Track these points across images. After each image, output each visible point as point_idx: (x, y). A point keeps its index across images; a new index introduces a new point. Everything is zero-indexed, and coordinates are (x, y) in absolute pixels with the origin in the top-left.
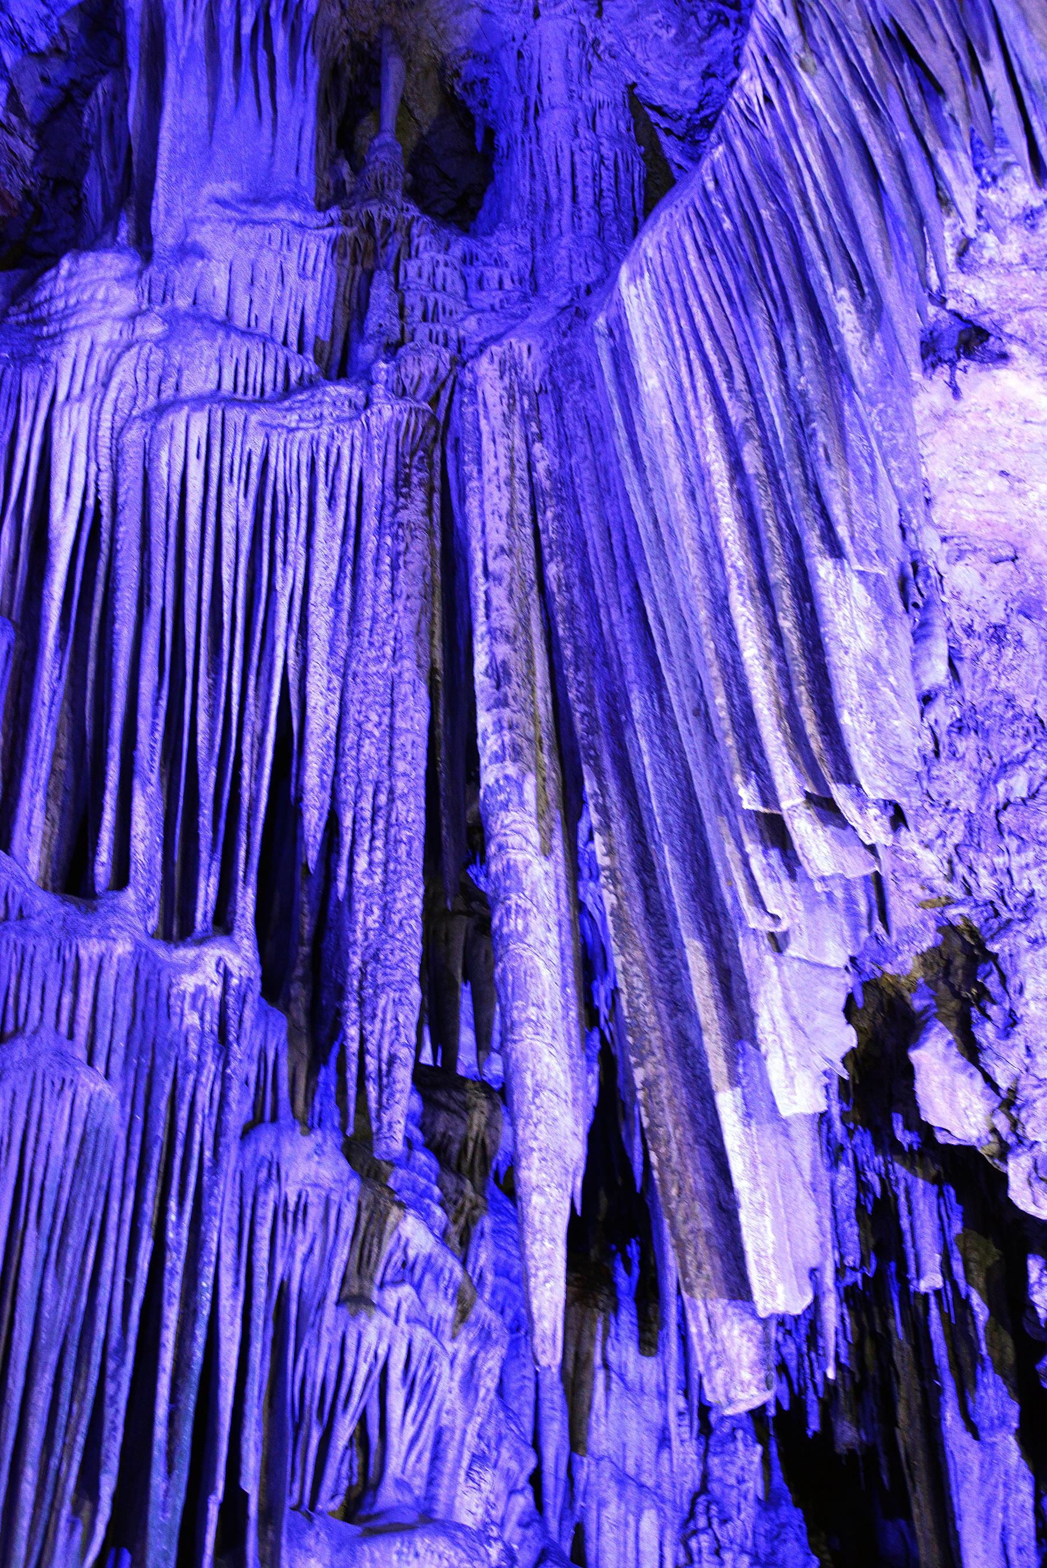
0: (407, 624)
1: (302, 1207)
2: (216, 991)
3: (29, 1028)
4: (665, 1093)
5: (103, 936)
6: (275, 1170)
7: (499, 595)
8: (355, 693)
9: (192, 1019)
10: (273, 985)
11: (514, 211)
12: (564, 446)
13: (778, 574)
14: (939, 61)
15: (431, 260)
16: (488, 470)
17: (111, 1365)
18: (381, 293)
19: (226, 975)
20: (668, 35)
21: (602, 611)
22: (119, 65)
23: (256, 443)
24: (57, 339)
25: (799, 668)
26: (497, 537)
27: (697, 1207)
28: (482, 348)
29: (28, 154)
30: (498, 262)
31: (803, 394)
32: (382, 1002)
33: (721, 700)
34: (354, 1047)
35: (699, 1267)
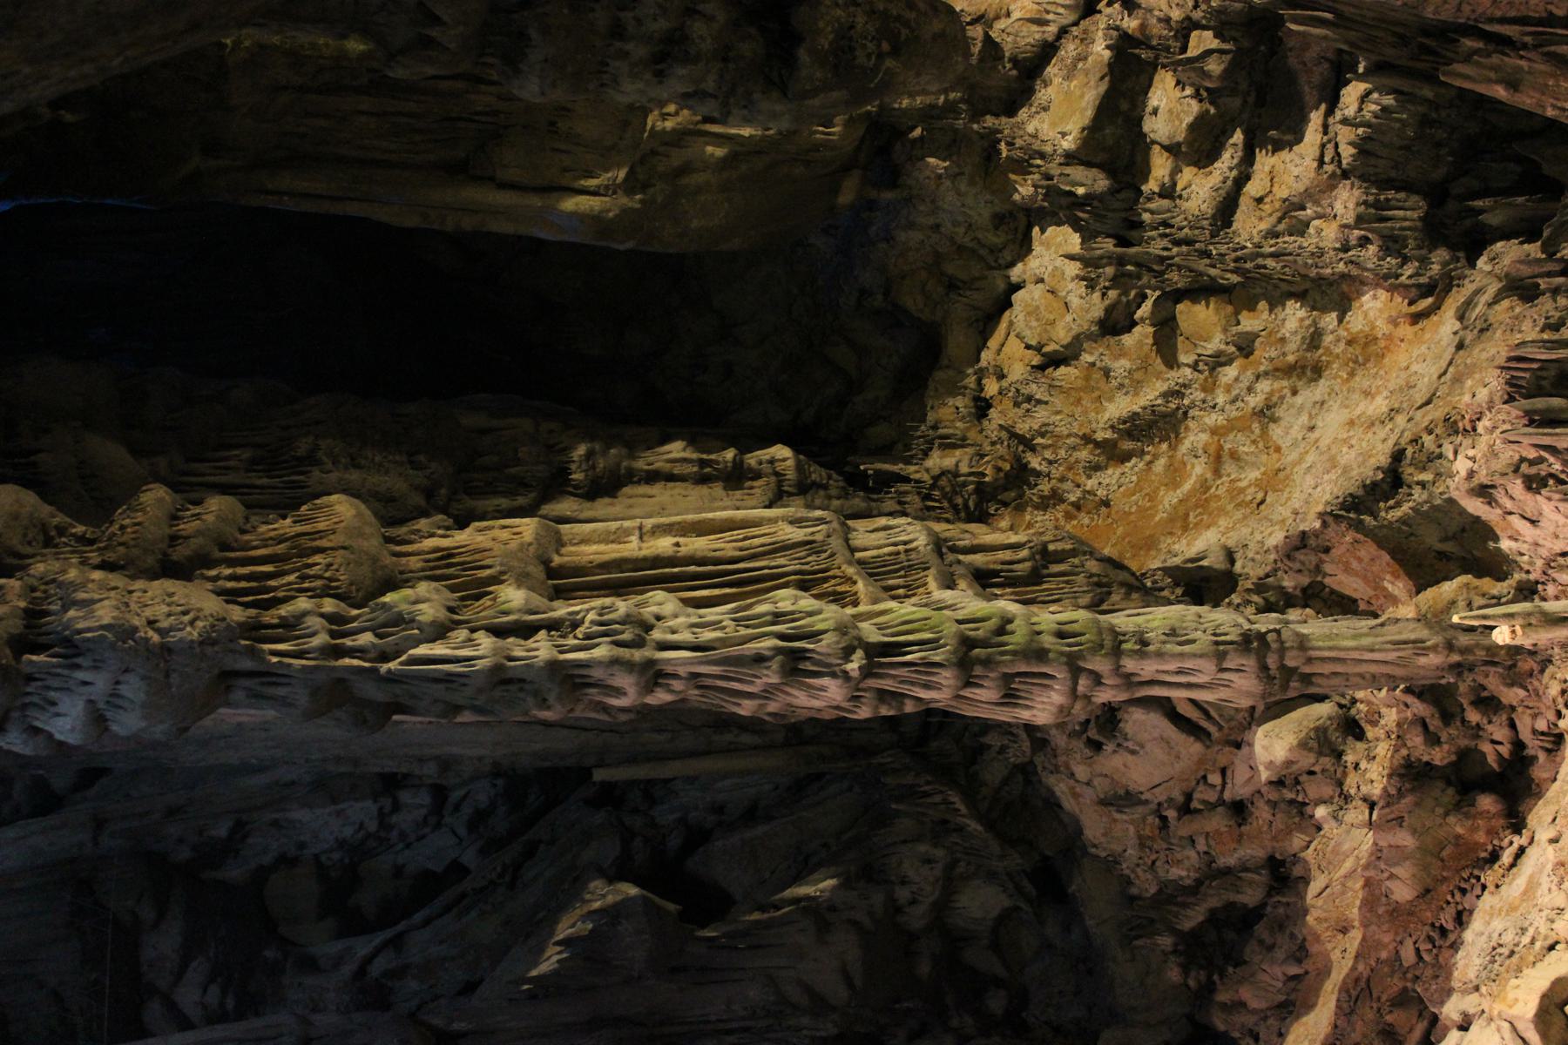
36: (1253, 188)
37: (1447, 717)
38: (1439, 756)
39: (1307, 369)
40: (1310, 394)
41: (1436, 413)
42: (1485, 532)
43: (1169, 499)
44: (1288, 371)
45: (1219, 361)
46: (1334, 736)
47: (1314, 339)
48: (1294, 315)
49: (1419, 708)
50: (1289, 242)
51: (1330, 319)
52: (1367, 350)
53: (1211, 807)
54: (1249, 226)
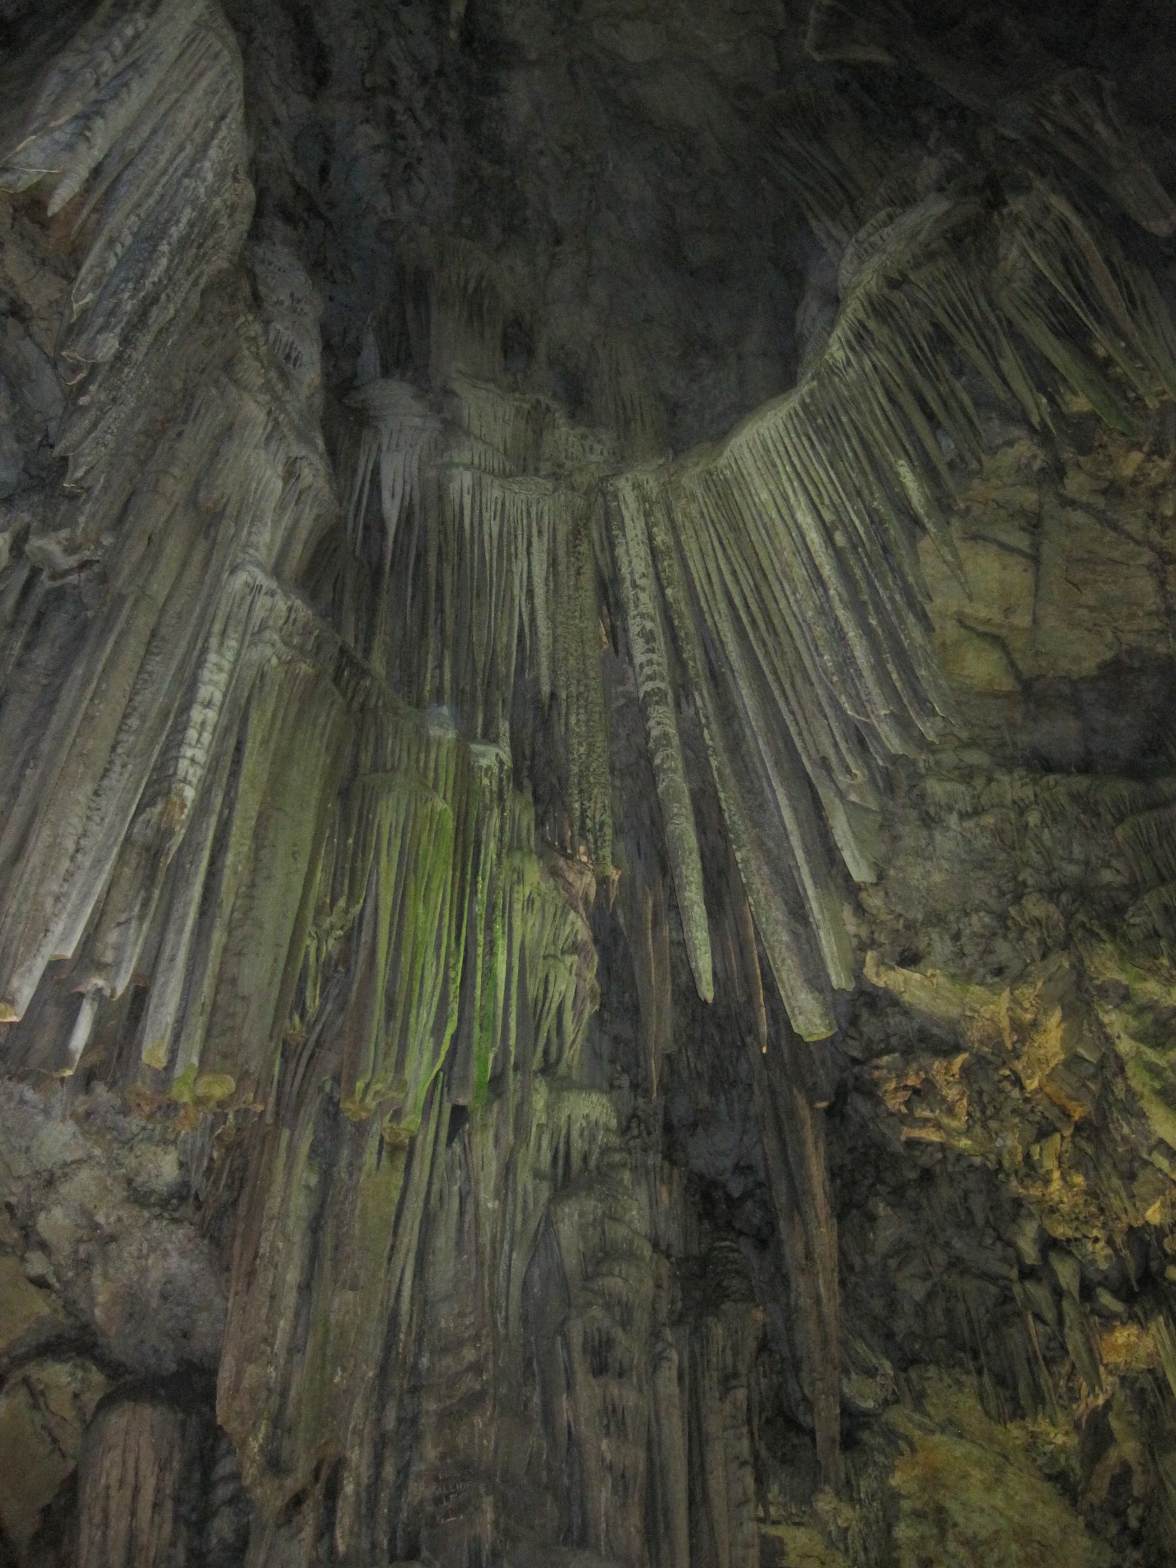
2: (496, 770)
3: (403, 767)
4: (754, 868)
9: (486, 782)
16: (630, 534)
17: (452, 961)
19: (501, 763)
21: (707, 616)
27: (780, 928)
31: (876, 510)
32: (596, 791)
34: (578, 813)
35: (783, 960)
39: (939, 1517)
40: (956, 1512)
47: (919, 1515)
48: (903, 1531)
51: (906, 1505)
52: (932, 1480)
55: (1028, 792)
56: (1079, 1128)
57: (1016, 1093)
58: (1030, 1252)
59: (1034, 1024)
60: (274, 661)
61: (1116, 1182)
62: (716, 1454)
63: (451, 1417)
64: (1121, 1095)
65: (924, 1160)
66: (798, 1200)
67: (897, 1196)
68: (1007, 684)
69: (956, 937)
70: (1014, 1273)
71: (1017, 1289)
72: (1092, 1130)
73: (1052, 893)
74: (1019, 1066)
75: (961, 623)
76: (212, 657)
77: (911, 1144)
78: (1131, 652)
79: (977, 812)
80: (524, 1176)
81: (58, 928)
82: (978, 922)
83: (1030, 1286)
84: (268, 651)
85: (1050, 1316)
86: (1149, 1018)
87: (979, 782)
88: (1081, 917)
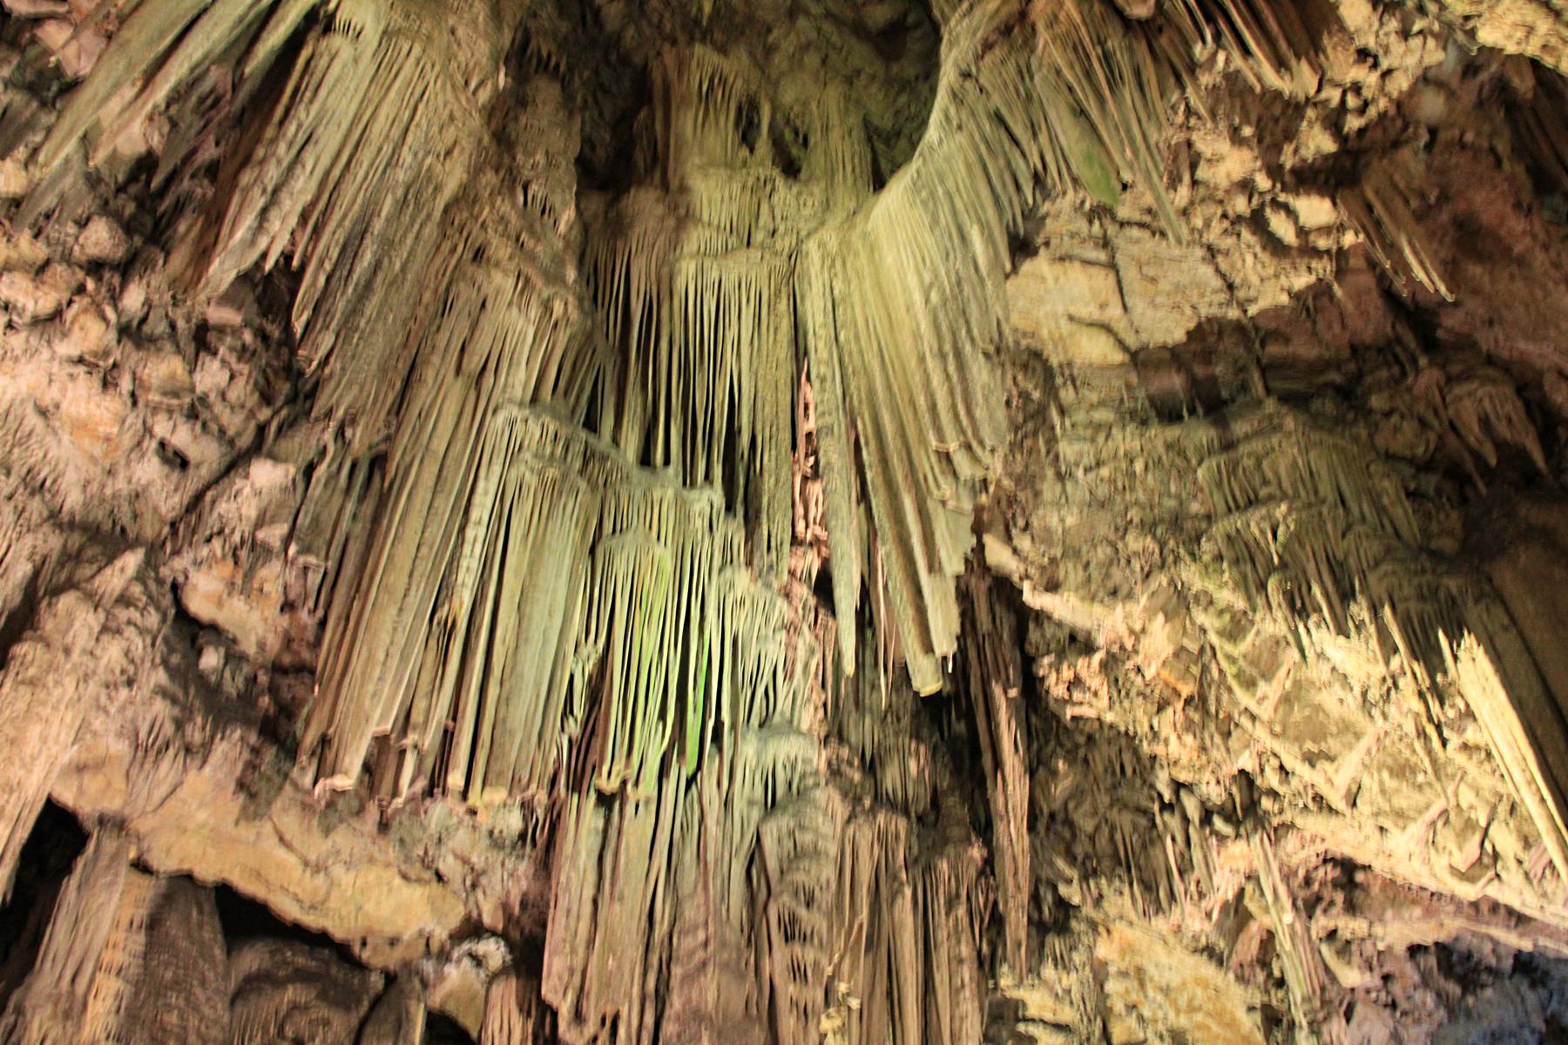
0: (782, 356)
1: (743, 602)
5: (663, 486)
6: (732, 585)
7: (821, 345)
8: (760, 384)
9: (699, 522)
10: (730, 507)
11: (818, 173)
12: (847, 281)
13: (948, 347)
14: (1019, 131)
15: (784, 193)
18: (765, 208)
20: (880, 97)
22: (650, 100)
23: (715, 275)
24: (631, 225)
25: (958, 390)
26: (820, 319)
28: (809, 235)
29: (608, 137)
30: (812, 195)
33: (922, 398)
36: (1048, 1016)
37: (1319, 899)
38: (1339, 897)
40: (1151, 970)
41: (1171, 940)
42: (1225, 907)
43: (1215, 1028)
44: (1142, 985)
45: (1141, 1019)
46: (1339, 944)
47: (1124, 974)
48: (1112, 986)
49: (1319, 911)
50: (1076, 996)
51: (1112, 969)
52: (1127, 949)
53: (1388, 993)
54: (1067, 1015)
55: (1137, 444)
56: (1188, 701)
57: (1139, 679)
58: (1167, 796)
59: (1143, 630)
60: (528, 474)
61: (1218, 739)
62: (941, 957)
63: (688, 979)
64: (1215, 674)
65: (1087, 729)
66: (998, 764)
67: (1071, 757)
68: (1118, 357)
69: (1087, 565)
70: (1156, 807)
71: (1158, 820)
72: (1198, 701)
73: (1148, 527)
74: (1139, 660)
75: (1071, 318)
76: (481, 484)
77: (1074, 718)
78: (1209, 320)
79: (1098, 464)
80: (739, 805)
81: (376, 716)
82: (1103, 552)
83: (1167, 816)
84: (522, 468)
85: (1180, 838)
86: (1227, 617)
87: (1101, 439)
88: (1172, 543)
